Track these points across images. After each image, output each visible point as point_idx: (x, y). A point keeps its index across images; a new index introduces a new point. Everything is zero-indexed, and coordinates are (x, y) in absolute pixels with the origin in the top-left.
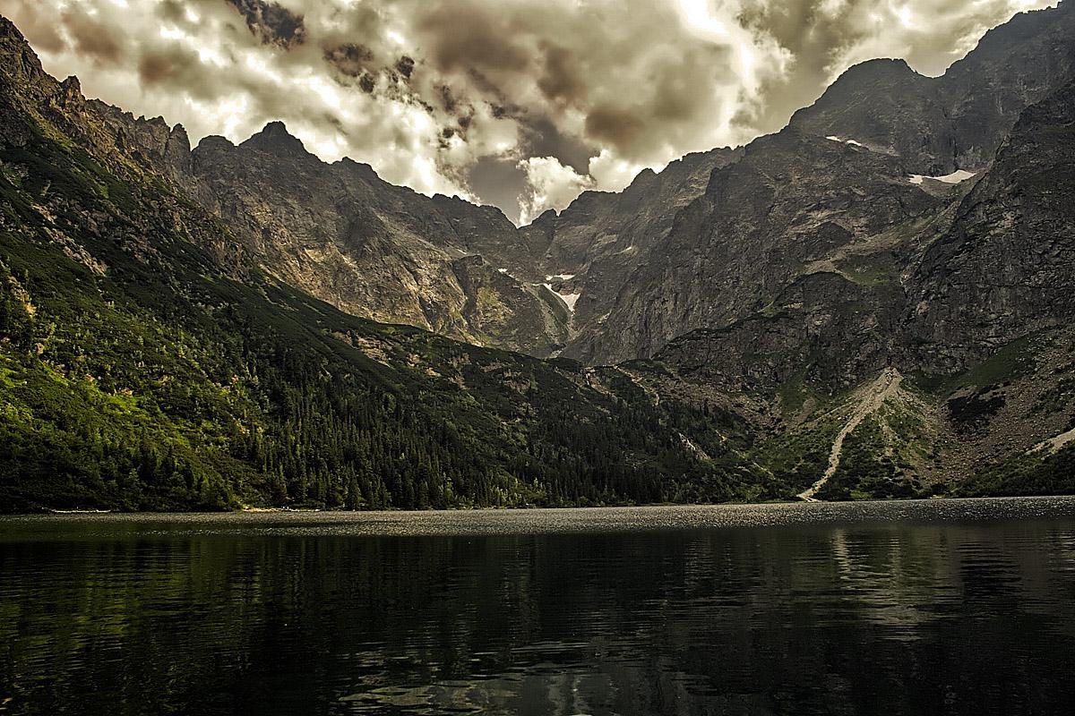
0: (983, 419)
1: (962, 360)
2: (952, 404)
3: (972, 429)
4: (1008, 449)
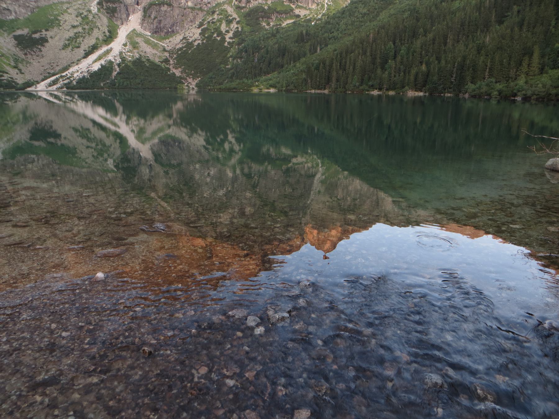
0: (37, 48)
1: (16, 13)
2: (16, 38)
3: (33, 53)
4: (57, 66)
